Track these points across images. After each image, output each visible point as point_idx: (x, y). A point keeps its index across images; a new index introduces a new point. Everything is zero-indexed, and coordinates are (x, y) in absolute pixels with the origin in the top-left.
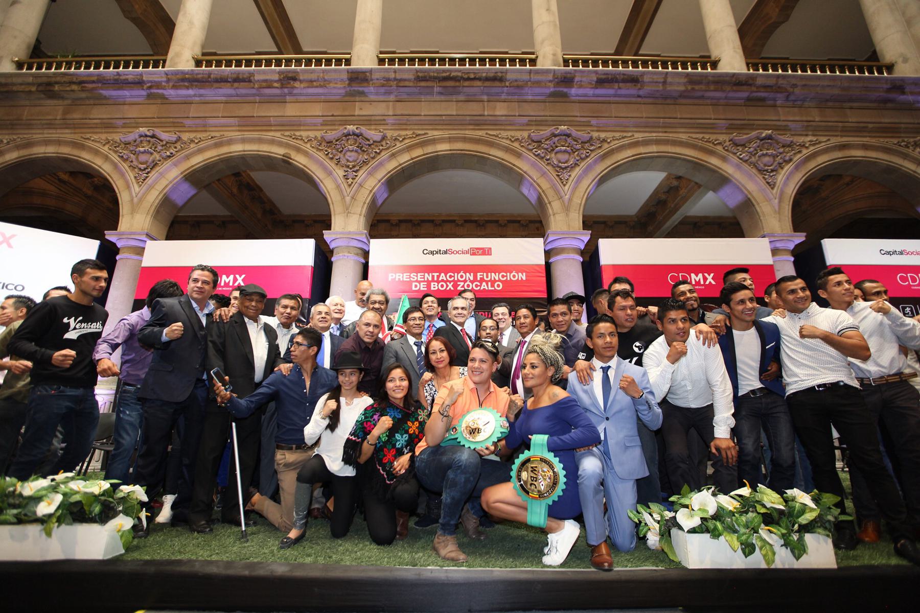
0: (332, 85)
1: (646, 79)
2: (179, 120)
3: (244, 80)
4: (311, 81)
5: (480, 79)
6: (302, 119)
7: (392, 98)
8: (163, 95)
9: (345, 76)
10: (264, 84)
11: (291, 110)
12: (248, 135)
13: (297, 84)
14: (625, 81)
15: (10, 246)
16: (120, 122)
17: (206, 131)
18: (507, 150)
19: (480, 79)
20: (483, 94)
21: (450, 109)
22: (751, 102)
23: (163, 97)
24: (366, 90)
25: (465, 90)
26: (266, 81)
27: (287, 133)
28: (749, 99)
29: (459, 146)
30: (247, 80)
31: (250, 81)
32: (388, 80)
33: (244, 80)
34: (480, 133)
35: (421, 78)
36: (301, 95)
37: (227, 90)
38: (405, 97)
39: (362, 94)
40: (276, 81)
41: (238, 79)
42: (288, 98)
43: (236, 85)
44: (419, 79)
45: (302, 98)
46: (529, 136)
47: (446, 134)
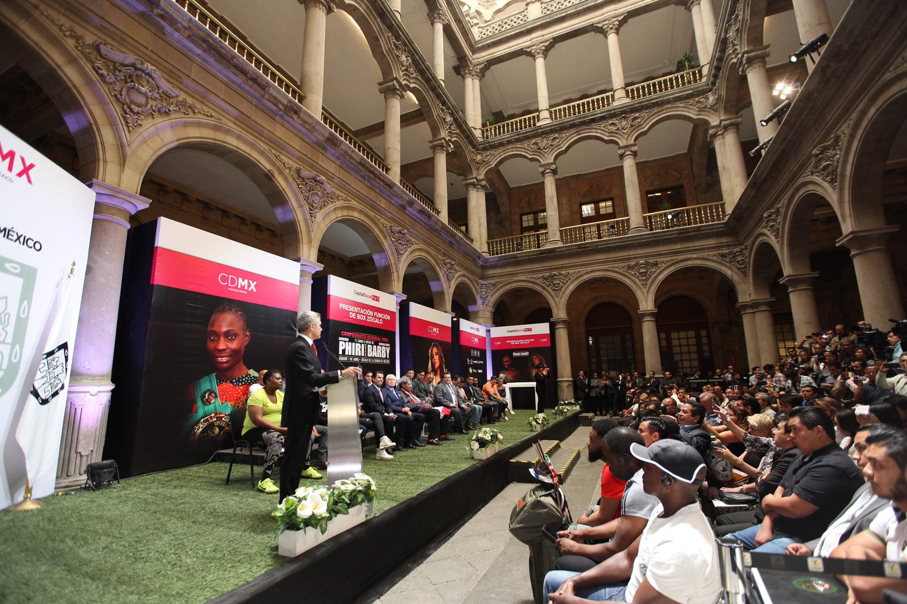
0: (316, 134)
1: (433, 218)
2: (177, 72)
3: (259, 85)
4: (305, 122)
5: (384, 182)
6: (287, 146)
7: (338, 162)
8: (163, 28)
9: (327, 135)
10: (273, 100)
11: (280, 132)
12: (245, 134)
13: (295, 117)
14: (367, 168)
15: (32, 166)
16: (97, 20)
17: (203, 103)
18: (381, 231)
19: (384, 182)
20: (378, 188)
21: (363, 189)
22: (451, 244)
23: (161, 30)
24: (329, 148)
25: (374, 182)
26: (275, 98)
27: (273, 151)
28: (450, 242)
29: (363, 218)
30: (264, 87)
31: (264, 89)
32: (346, 153)
33: (259, 85)
34: (373, 214)
35: (362, 164)
36: (288, 122)
37: (239, 79)
38: (344, 166)
39: (325, 149)
40: (283, 104)
41: (255, 80)
42: (277, 118)
43: (250, 82)
44: (361, 164)
45: (287, 125)
46: (391, 227)
47: (360, 207)
